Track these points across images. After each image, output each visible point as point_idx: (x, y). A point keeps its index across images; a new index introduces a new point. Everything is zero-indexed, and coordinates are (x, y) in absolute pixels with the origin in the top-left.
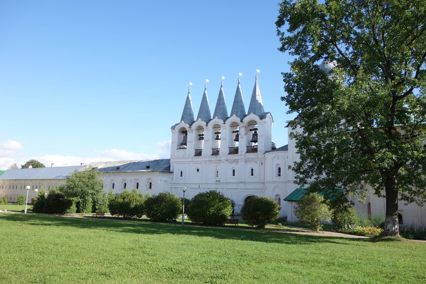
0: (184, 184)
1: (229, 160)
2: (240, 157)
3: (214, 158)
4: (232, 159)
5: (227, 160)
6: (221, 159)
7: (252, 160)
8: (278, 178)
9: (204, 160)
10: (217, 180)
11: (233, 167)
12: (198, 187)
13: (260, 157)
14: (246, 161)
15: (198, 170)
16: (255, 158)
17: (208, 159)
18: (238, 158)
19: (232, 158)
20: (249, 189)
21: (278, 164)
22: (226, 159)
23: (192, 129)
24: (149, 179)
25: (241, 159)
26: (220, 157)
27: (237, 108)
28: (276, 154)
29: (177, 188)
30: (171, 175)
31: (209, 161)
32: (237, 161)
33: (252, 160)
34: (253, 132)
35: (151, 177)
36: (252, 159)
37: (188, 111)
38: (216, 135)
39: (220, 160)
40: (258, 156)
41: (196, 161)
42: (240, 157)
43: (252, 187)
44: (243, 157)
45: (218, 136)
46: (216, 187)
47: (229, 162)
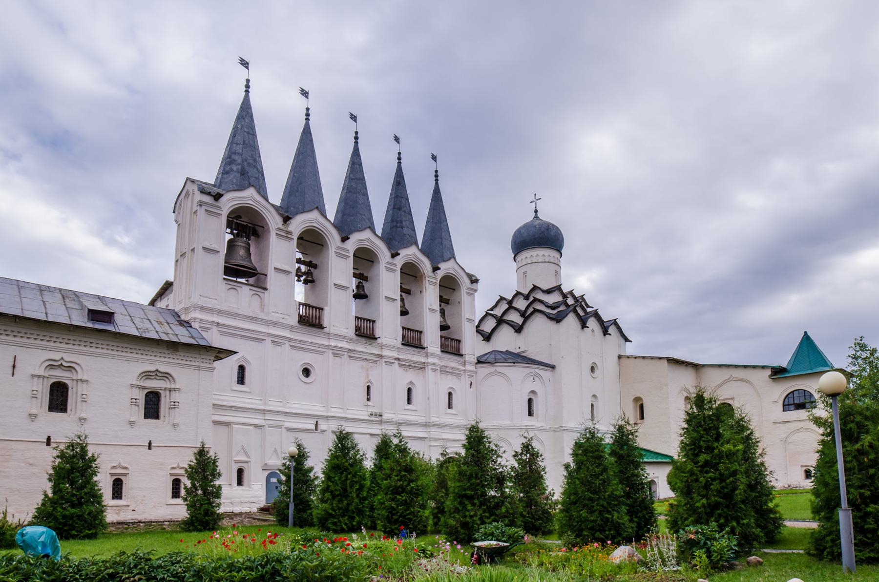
0: (264, 411)
1: (404, 360)
2: (431, 360)
3: (362, 347)
4: (410, 361)
5: (398, 359)
6: (385, 353)
9: (333, 343)
11: (411, 383)
14: (444, 370)
15: (307, 372)
16: (458, 369)
17: (347, 346)
18: (425, 360)
24: (147, 375)
25: (434, 364)
26: (382, 347)
29: (227, 424)
32: (421, 367)
35: (163, 368)
36: (453, 368)
39: (381, 356)
42: (431, 360)
47: (401, 365)
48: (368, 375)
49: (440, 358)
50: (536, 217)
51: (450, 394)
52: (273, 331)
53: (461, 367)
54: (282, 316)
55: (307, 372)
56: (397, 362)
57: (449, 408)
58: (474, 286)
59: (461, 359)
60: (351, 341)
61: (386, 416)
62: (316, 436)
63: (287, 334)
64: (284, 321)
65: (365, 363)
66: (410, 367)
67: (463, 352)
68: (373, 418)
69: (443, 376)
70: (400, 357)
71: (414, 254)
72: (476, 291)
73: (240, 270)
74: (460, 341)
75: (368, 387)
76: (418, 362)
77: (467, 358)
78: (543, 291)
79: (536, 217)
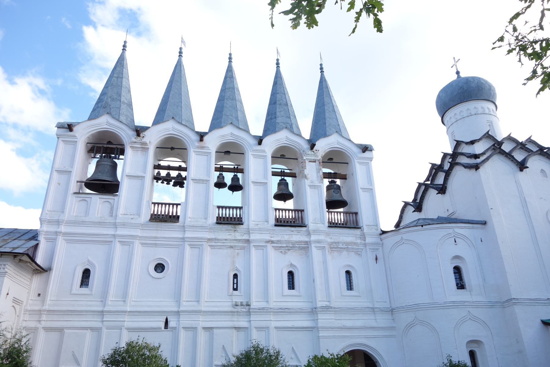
1: (279, 242)
3: (226, 233)
4: (288, 242)
5: (272, 242)
6: (253, 237)
7: (347, 247)
8: (462, 295)
10: (239, 300)
11: (292, 265)
12: (163, 325)
13: (369, 240)
14: (335, 247)
16: (355, 244)
19: (286, 238)
20: (350, 328)
21: (457, 257)
22: (267, 237)
23: (145, 140)
25: (319, 242)
27: (290, 118)
28: (451, 231)
29: (61, 330)
30: (37, 281)
31: (209, 240)
33: (347, 247)
34: (326, 182)
36: (347, 244)
37: (123, 94)
38: (218, 173)
40: (363, 237)
41: (156, 237)
43: (359, 324)
44: (322, 237)
45: (223, 177)
46: (237, 324)
47: (276, 248)
48: (234, 263)
49: (328, 234)
50: (459, 76)
51: (348, 273)
52: (120, 232)
53: (359, 241)
54: (132, 217)
55: (160, 268)
56: (269, 246)
57: (348, 290)
58: (367, 154)
59: (358, 232)
60: (210, 230)
61: (254, 304)
62: (167, 334)
63: (139, 233)
64: (132, 221)
65: (230, 251)
66: (289, 249)
67: (361, 225)
68: (239, 309)
69: (336, 254)
70: (273, 239)
71: (287, 138)
72: (371, 159)
73: (104, 185)
74: (356, 214)
75: (235, 276)
76: (297, 242)
77: (366, 229)
78: (467, 143)
79: (459, 76)
